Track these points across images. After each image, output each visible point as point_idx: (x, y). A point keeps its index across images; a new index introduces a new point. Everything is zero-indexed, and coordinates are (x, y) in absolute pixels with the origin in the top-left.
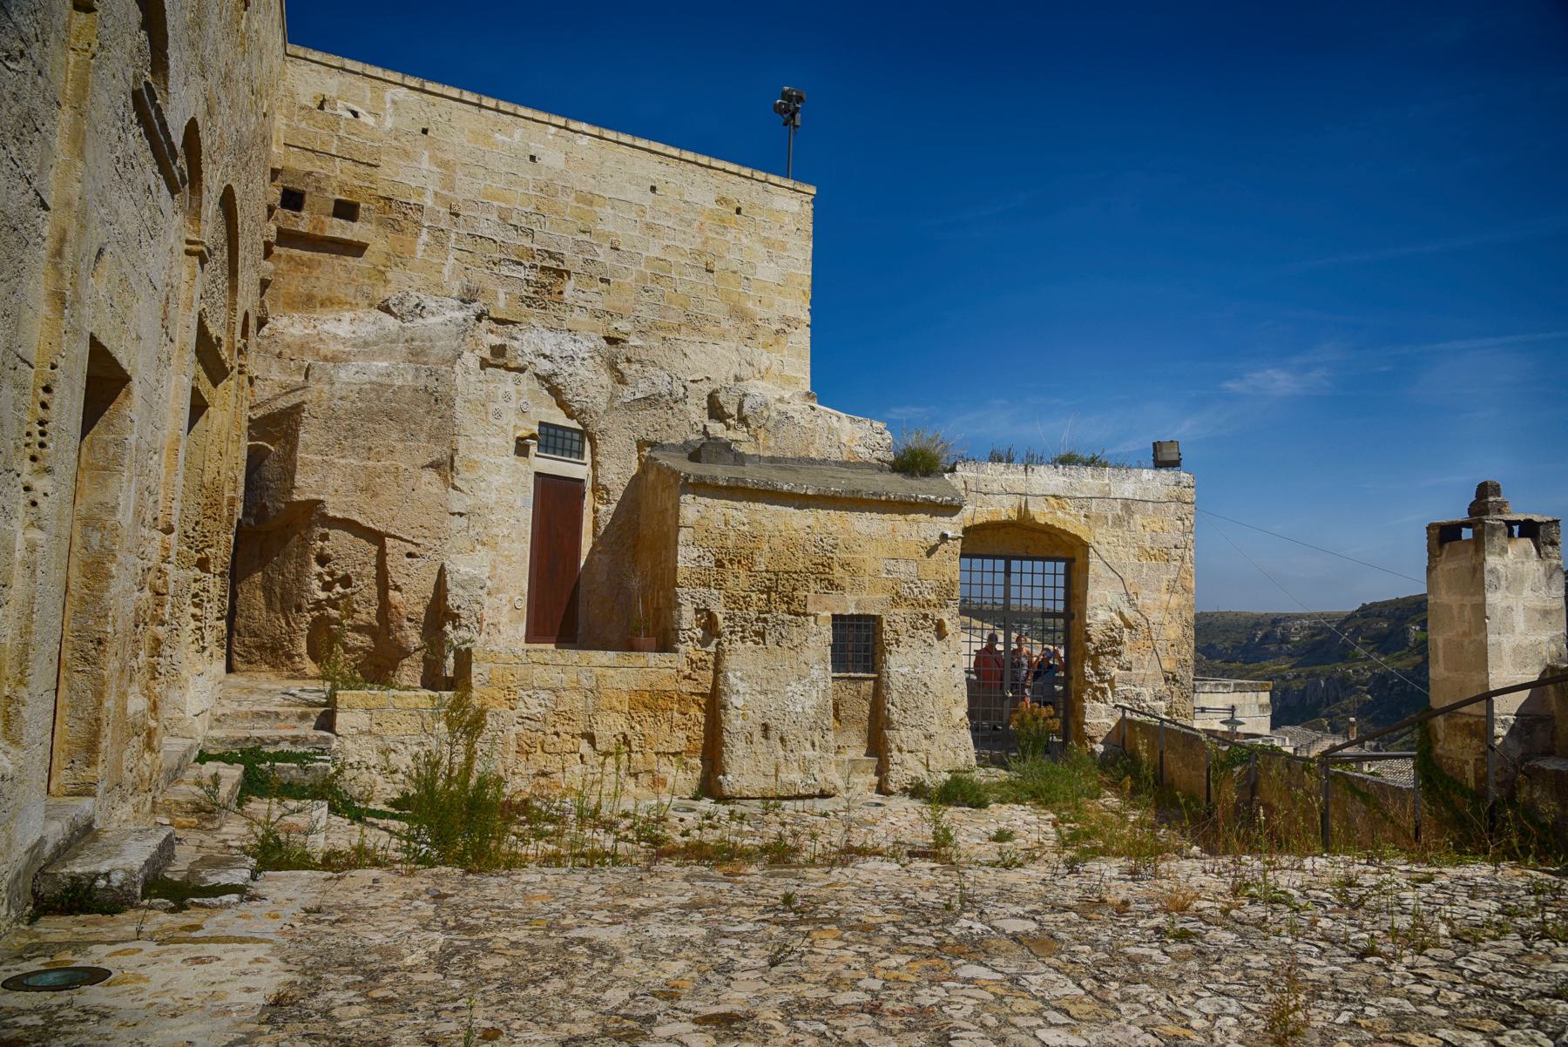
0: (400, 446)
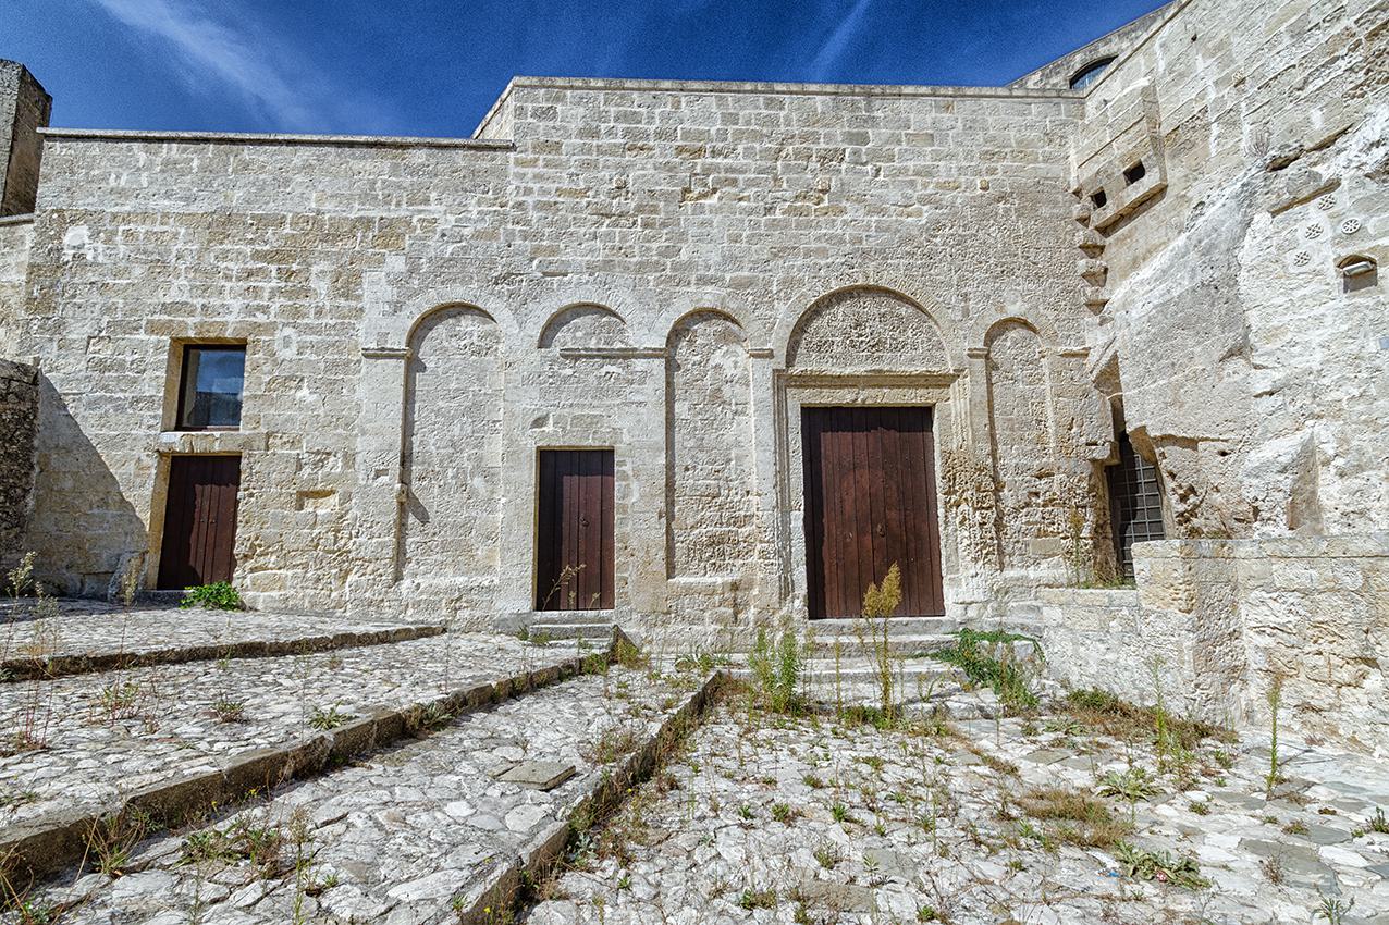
0: (1198, 349)
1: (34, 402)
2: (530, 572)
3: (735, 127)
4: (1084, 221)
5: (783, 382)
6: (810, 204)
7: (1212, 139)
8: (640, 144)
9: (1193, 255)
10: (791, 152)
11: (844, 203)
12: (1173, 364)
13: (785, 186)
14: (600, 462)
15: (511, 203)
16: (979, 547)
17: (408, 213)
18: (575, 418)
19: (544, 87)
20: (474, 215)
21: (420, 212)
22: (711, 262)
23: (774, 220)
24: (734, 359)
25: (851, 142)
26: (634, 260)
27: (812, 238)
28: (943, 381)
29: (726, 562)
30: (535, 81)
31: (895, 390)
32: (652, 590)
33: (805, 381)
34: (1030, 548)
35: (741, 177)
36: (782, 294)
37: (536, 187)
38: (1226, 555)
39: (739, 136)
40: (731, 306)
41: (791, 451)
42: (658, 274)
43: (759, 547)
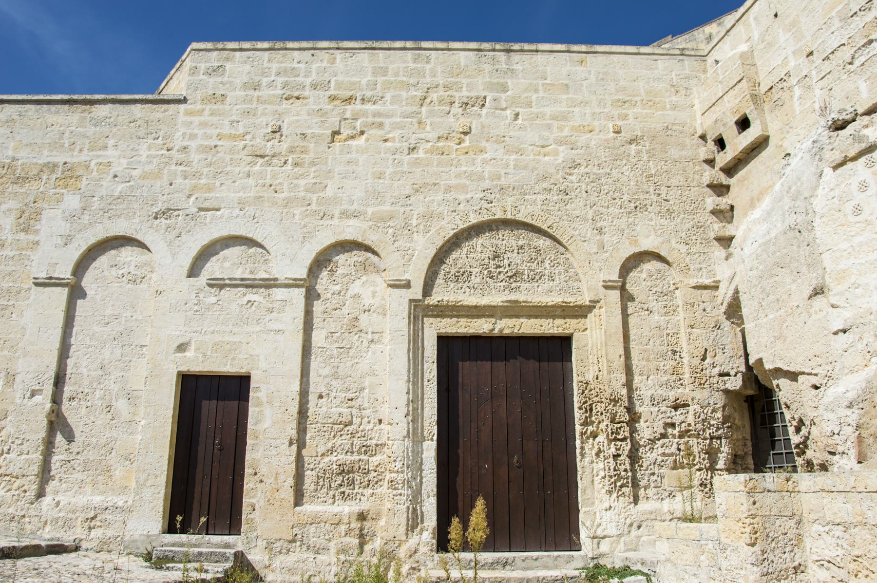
0: (793, 287)
2: (162, 495)
3: (384, 78)
4: (711, 162)
5: (419, 311)
6: (452, 144)
7: (795, 99)
8: (296, 94)
9: (787, 200)
10: (435, 99)
11: (484, 144)
12: (778, 300)
13: (428, 128)
14: (236, 388)
15: (176, 148)
16: (613, 480)
17: (88, 159)
18: (216, 344)
19: (217, 49)
20: (144, 159)
21: (98, 157)
22: (354, 198)
23: (417, 159)
24: (372, 289)
25: (491, 90)
26: (282, 196)
27: (453, 176)
28: (581, 312)
29: (355, 492)
30: (209, 45)
31: (532, 320)
32: (278, 517)
33: (442, 311)
34: (665, 481)
35: (387, 121)
36: (422, 227)
37: (200, 132)
38: (790, 489)
39: (388, 86)
40: (370, 239)
41: (426, 380)
42: (304, 209)
43: (388, 476)
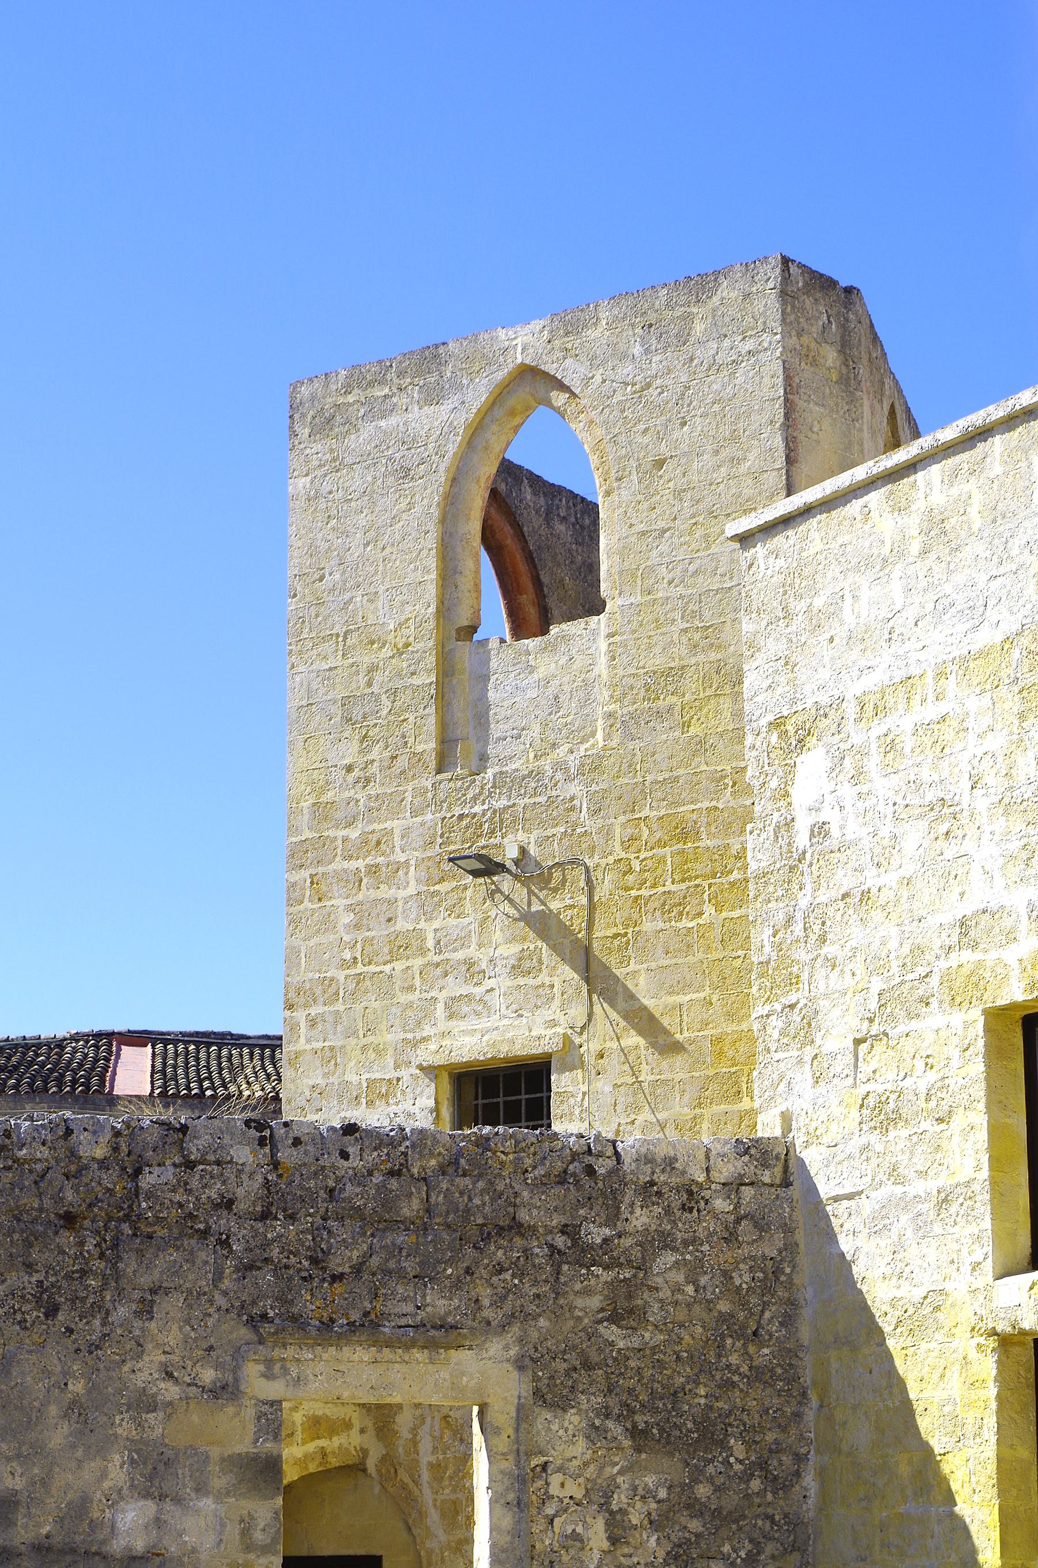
1: (788, 1230)
